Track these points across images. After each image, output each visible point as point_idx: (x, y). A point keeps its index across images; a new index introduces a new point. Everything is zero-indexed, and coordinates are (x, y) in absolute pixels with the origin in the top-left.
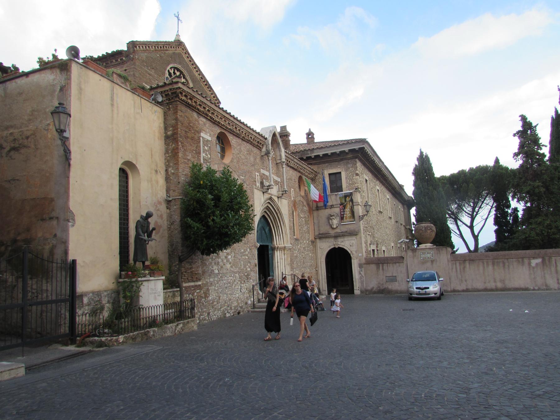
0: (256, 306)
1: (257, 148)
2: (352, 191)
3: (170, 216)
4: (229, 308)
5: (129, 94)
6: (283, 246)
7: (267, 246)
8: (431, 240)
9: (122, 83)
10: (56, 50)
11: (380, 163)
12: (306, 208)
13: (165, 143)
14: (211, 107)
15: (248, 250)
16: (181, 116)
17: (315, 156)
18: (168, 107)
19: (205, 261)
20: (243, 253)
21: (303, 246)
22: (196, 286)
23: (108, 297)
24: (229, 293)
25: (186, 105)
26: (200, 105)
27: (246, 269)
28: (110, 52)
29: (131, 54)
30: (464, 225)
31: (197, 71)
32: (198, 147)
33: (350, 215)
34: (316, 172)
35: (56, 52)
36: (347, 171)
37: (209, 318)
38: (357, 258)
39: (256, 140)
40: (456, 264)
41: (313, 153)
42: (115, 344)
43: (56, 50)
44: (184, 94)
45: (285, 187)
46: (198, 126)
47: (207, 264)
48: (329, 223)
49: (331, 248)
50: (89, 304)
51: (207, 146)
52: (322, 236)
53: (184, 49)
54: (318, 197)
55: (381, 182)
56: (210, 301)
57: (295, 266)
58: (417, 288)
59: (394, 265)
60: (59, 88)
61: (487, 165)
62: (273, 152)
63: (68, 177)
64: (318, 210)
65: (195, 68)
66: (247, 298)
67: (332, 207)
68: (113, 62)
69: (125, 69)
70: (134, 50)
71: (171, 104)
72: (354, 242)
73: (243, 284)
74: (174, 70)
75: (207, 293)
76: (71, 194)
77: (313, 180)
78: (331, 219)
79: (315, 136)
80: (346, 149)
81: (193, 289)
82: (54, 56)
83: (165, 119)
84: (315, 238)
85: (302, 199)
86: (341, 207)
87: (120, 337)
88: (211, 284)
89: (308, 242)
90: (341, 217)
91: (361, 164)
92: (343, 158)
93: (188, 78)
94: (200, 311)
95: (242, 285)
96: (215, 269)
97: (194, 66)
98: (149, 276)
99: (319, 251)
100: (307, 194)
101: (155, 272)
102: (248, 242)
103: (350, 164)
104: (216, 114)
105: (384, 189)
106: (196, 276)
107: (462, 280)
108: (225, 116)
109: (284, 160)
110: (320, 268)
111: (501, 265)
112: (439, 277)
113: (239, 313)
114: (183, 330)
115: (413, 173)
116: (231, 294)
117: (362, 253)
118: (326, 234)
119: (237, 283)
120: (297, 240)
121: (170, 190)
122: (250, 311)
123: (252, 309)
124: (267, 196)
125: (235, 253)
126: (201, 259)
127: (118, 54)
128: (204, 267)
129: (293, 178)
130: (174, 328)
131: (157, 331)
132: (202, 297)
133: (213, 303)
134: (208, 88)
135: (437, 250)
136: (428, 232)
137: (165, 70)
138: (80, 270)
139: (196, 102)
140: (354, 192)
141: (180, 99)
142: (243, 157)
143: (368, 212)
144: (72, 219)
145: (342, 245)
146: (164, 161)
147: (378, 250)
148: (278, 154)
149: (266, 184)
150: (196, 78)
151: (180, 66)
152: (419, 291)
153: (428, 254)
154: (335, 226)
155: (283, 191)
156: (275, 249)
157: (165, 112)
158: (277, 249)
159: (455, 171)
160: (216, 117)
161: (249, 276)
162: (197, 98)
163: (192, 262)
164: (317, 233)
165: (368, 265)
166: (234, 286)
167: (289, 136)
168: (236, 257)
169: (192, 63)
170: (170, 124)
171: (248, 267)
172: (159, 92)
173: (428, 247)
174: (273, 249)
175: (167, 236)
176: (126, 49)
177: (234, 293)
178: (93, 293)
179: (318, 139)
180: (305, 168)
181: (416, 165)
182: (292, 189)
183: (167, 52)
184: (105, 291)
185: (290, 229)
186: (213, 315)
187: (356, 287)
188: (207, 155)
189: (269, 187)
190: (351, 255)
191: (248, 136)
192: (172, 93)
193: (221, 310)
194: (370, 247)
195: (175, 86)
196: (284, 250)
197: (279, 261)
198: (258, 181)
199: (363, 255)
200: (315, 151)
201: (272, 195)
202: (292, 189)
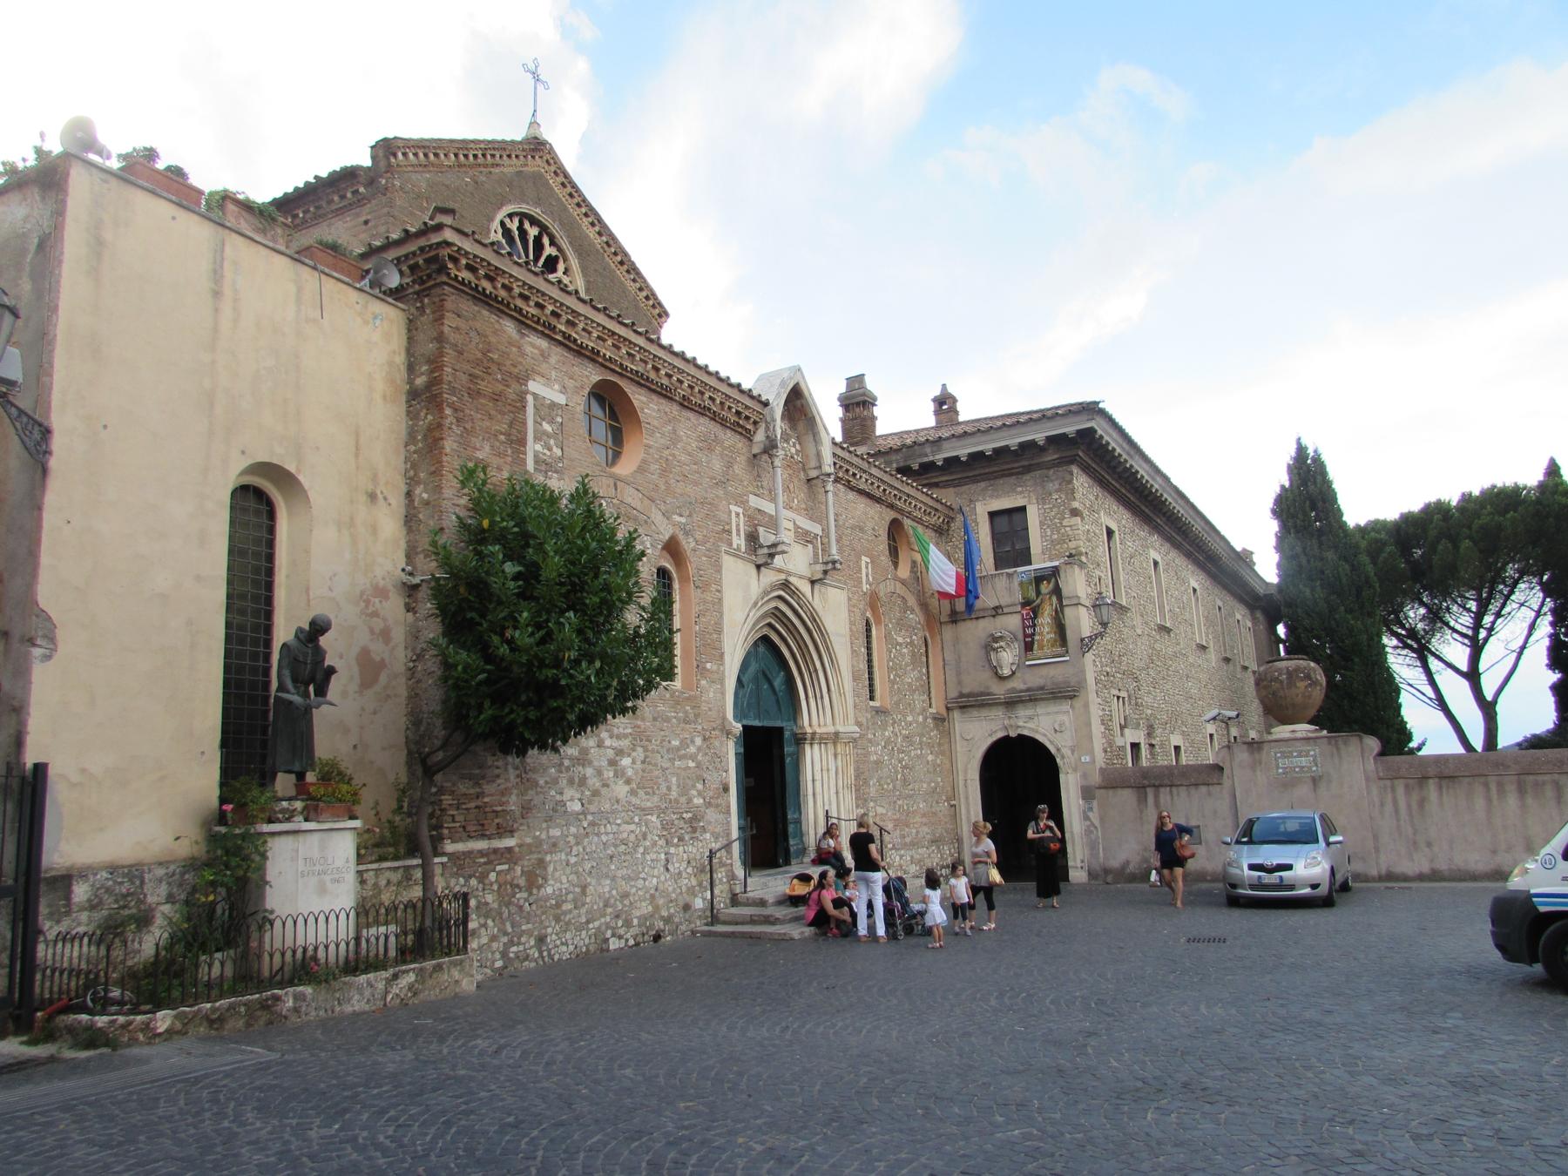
0: (722, 917)
1: (736, 431)
2: (1056, 563)
3: (414, 634)
4: (620, 923)
5: (281, 262)
6: (831, 729)
7: (780, 730)
8: (1312, 712)
9: (258, 230)
10: (42, 135)
11: (1154, 479)
12: (916, 617)
13: (408, 413)
14: (562, 304)
15: (698, 741)
16: (457, 329)
17: (946, 460)
18: (418, 305)
19: (531, 775)
20: (678, 749)
21: (904, 732)
22: (495, 851)
23: (169, 884)
24: (619, 873)
25: (474, 297)
26: (525, 298)
27: (690, 801)
28: (324, 174)
29: (381, 177)
30: (1449, 670)
31: (593, 224)
32: (518, 424)
33: (1052, 635)
34: (950, 508)
35: (43, 140)
36: (1044, 504)
37: (541, 952)
38: (1075, 770)
39: (730, 408)
40: (1393, 789)
41: (940, 450)
42: (141, 1037)
43: (42, 135)
44: (464, 262)
45: (834, 550)
46: (520, 359)
47: (541, 782)
48: (990, 661)
49: (994, 738)
50: (92, 906)
51: (551, 422)
52: (969, 702)
53: (552, 161)
54: (953, 582)
55: (1168, 539)
56: (547, 898)
57: (873, 791)
58: (1252, 867)
59: (1193, 790)
60: (36, 241)
61: (1516, 484)
62: (794, 446)
63: (40, 508)
64: (954, 622)
65: (586, 215)
66: (692, 892)
67: (997, 611)
68: (332, 201)
69: (364, 218)
70: (389, 165)
71: (427, 295)
72: (1065, 718)
73: (677, 846)
74: (521, 223)
75: (537, 876)
76: (45, 559)
77: (941, 534)
78: (995, 650)
79: (959, 407)
80: (1039, 435)
81: (482, 860)
82: (39, 151)
83: (410, 340)
84: (948, 709)
85: (900, 589)
86: (1024, 612)
87: (160, 1014)
88: (554, 845)
89: (921, 719)
90: (1026, 643)
91: (1091, 482)
92: (1031, 465)
93: (565, 244)
94: (510, 930)
95: (672, 850)
96: (572, 800)
97: (584, 210)
98: (301, 818)
99: (960, 747)
100: (919, 574)
101: (321, 804)
102: (697, 716)
103: (1052, 481)
104: (581, 325)
105: (1179, 561)
106: (497, 821)
107: (1415, 843)
108: (614, 333)
109: (829, 469)
110: (962, 800)
111: (1549, 792)
112: (1330, 829)
113: (657, 938)
114: (415, 994)
115: (1274, 512)
116: (628, 879)
117: (1091, 752)
118: (982, 694)
119: (654, 844)
120: (879, 711)
121: (417, 553)
122: (698, 932)
123: (707, 925)
124: (769, 577)
125: (646, 750)
126: (517, 768)
127: (348, 175)
128: (530, 792)
129: (869, 525)
130: (381, 986)
131: (309, 997)
132: (518, 886)
133: (558, 905)
134: (628, 272)
135: (1330, 743)
136: (1296, 687)
137: (492, 220)
138: (60, 800)
139: (508, 289)
140: (1063, 567)
141: (451, 278)
142: (683, 458)
143: (1104, 625)
144: (44, 636)
145: (1030, 729)
146: (403, 466)
147: (1152, 746)
148: (811, 451)
149: (766, 537)
150: (592, 244)
151: (538, 210)
152: (1260, 877)
153: (1300, 756)
154: (1006, 672)
155: (826, 563)
156: (805, 739)
157: (410, 321)
158: (813, 739)
159: (1415, 505)
160: (584, 333)
161: (699, 821)
162: (511, 276)
163: (483, 777)
164: (953, 694)
165: (1111, 792)
166: (643, 854)
167: (874, 405)
168: (649, 763)
169: (576, 201)
170: (423, 355)
171: (694, 792)
172: (393, 260)
173: (1299, 735)
174: (800, 740)
175: (403, 692)
176: (367, 162)
177: (643, 875)
178: (113, 869)
179: (967, 412)
180: (908, 495)
181: (1283, 487)
182: (865, 559)
183: (497, 170)
184: (160, 864)
185: (855, 678)
186: (558, 942)
187: (1075, 860)
188: (550, 449)
189: (774, 550)
190: (1058, 760)
191: (702, 393)
192: (427, 261)
193: (588, 930)
194: (1122, 735)
195: (435, 239)
196: (835, 743)
197: (818, 776)
198: (738, 530)
199: (1093, 761)
200: (945, 445)
201: (789, 574)
202: (865, 559)
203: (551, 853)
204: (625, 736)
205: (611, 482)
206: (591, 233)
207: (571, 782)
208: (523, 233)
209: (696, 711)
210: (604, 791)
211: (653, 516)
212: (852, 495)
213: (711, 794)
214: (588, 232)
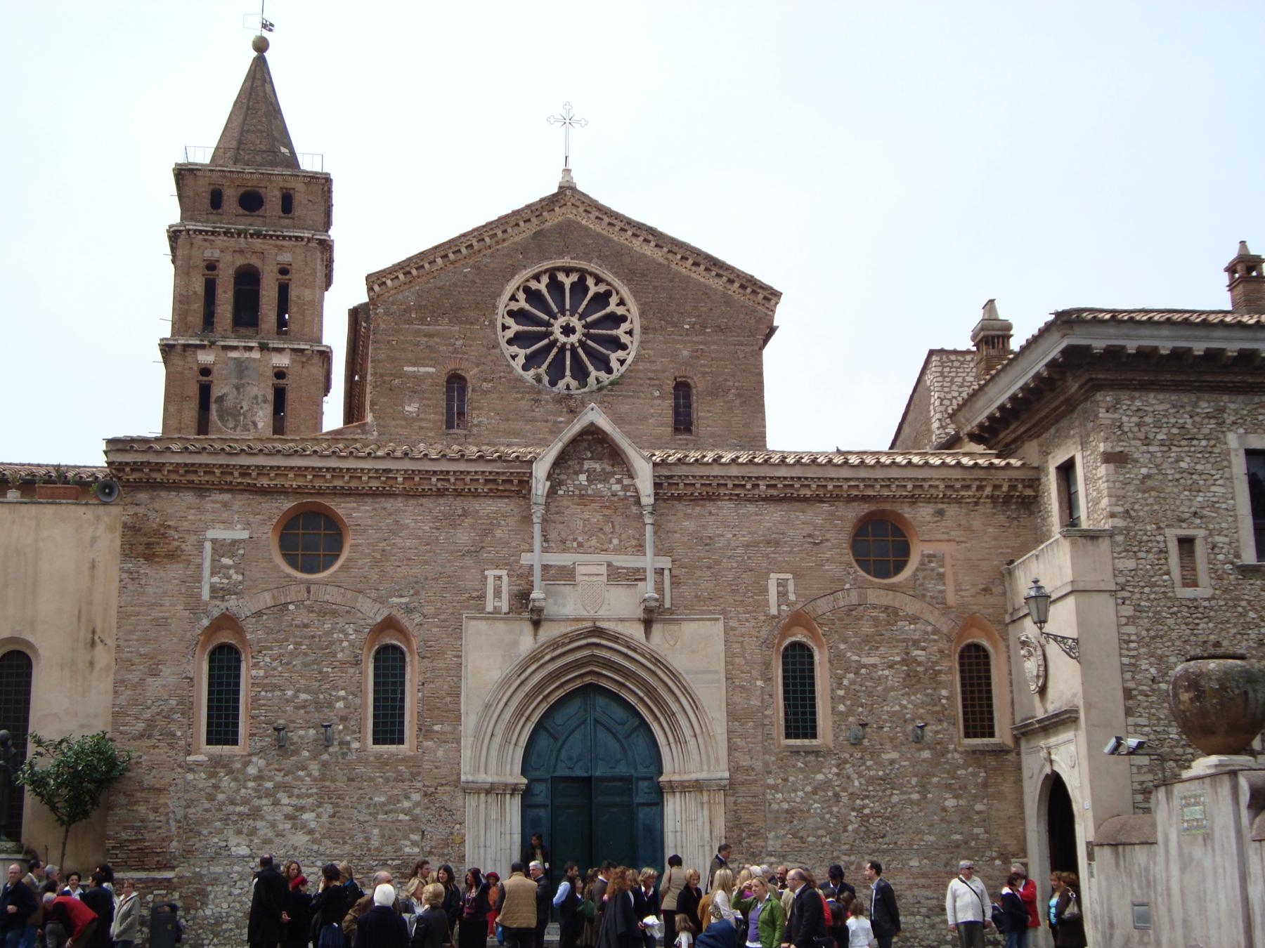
22: (154, 880)
47: (205, 832)
56: (206, 918)
62: (619, 481)
84: (1017, 740)
93: (608, 276)
96: (238, 845)
102: (414, 776)
176: (366, 299)
188: (229, 577)
201: (594, 620)
203: (212, 885)
204: (309, 796)
205: (303, 587)
206: (649, 250)
207: (239, 832)
208: (555, 286)
209: (415, 770)
210: (277, 840)
211: (358, 605)
212: (751, 508)
213: (433, 844)
214: (643, 251)
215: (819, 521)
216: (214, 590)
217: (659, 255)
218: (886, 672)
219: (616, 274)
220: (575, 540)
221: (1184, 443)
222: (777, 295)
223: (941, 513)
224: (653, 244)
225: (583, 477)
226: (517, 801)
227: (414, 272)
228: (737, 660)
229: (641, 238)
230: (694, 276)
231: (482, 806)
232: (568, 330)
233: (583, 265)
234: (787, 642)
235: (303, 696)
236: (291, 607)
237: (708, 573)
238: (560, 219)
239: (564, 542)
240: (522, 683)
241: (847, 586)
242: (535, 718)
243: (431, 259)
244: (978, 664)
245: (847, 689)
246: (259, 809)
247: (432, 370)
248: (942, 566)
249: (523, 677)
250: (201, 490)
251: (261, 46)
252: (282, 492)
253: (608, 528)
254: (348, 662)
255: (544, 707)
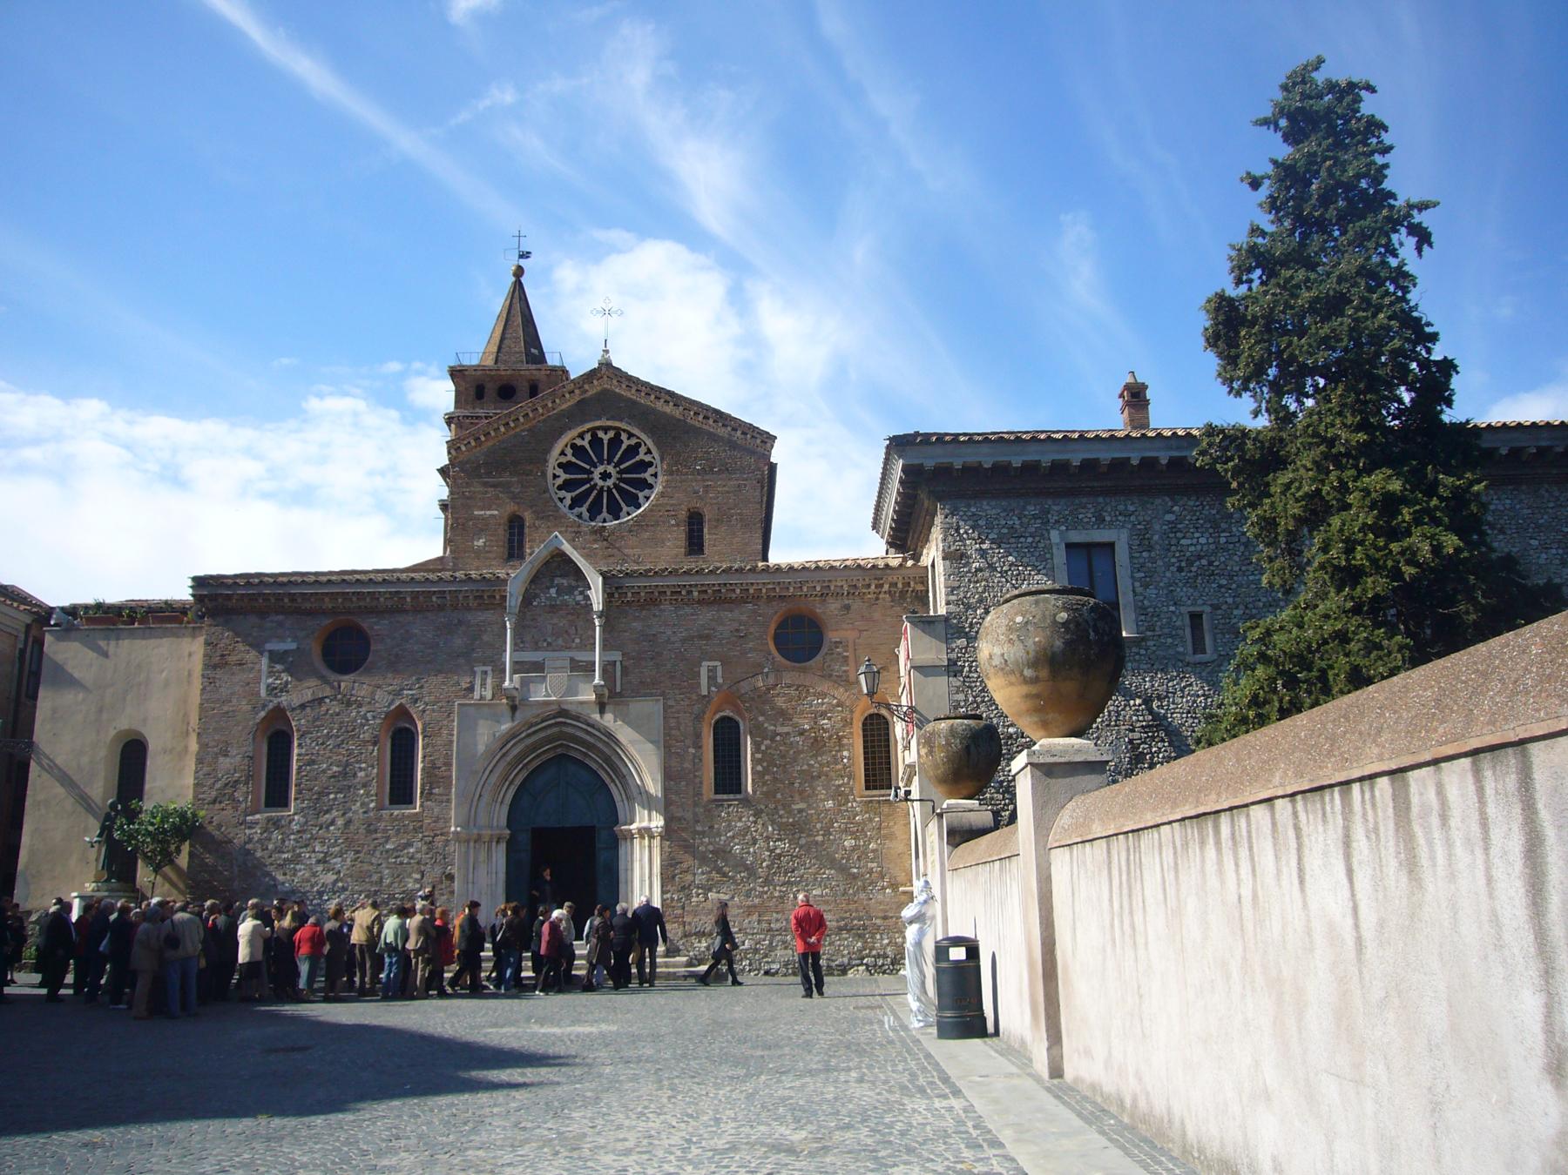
93: (636, 431)
176: (447, 462)
215: (744, 618)
216: (271, 690)
217: (678, 413)
218: (798, 739)
219: (643, 430)
220: (545, 640)
221: (1013, 540)
222: (776, 438)
223: (847, 608)
224: (671, 404)
225: (553, 591)
226: (503, 846)
227: (483, 439)
228: (673, 732)
229: (662, 400)
230: (704, 427)
231: (472, 851)
232: (605, 476)
233: (617, 424)
234: (717, 716)
235: (335, 769)
236: (327, 700)
237: (651, 663)
238: (599, 388)
239: (536, 643)
240: (504, 755)
241: (766, 670)
242: (518, 782)
243: (496, 426)
244: (872, 730)
245: (763, 753)
246: (299, 855)
247: (496, 512)
248: (847, 651)
249: (504, 750)
250: (263, 614)
251: (519, 272)
252: (324, 613)
253: (572, 631)
254: (368, 741)
255: (525, 774)
